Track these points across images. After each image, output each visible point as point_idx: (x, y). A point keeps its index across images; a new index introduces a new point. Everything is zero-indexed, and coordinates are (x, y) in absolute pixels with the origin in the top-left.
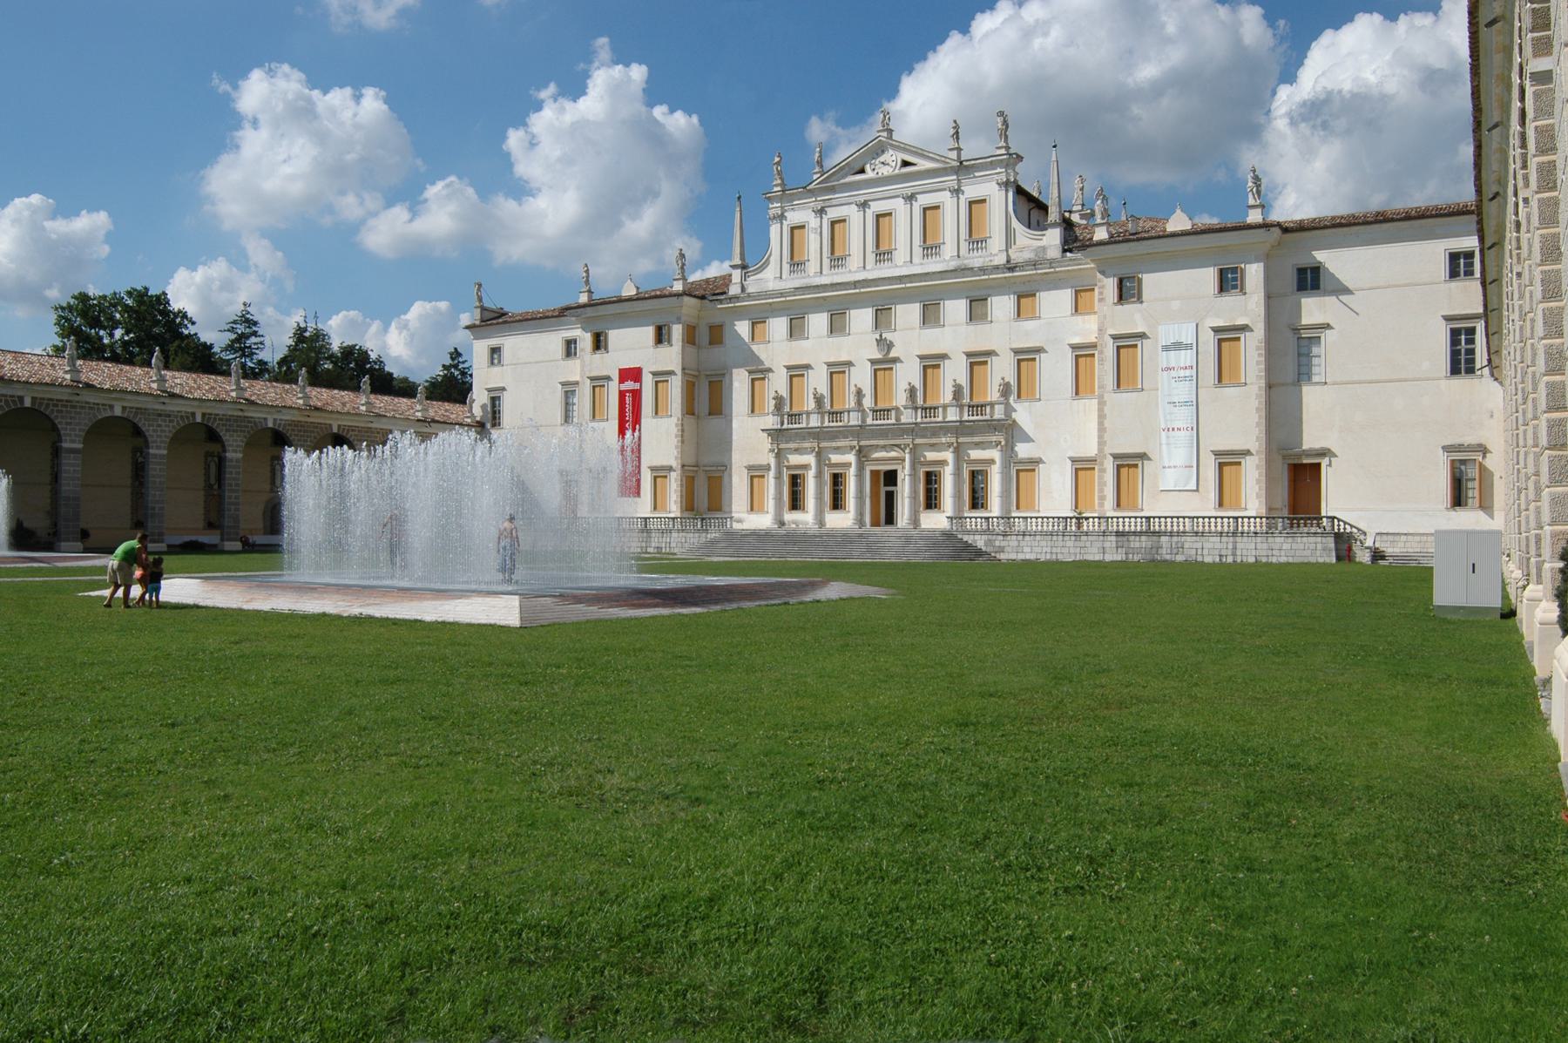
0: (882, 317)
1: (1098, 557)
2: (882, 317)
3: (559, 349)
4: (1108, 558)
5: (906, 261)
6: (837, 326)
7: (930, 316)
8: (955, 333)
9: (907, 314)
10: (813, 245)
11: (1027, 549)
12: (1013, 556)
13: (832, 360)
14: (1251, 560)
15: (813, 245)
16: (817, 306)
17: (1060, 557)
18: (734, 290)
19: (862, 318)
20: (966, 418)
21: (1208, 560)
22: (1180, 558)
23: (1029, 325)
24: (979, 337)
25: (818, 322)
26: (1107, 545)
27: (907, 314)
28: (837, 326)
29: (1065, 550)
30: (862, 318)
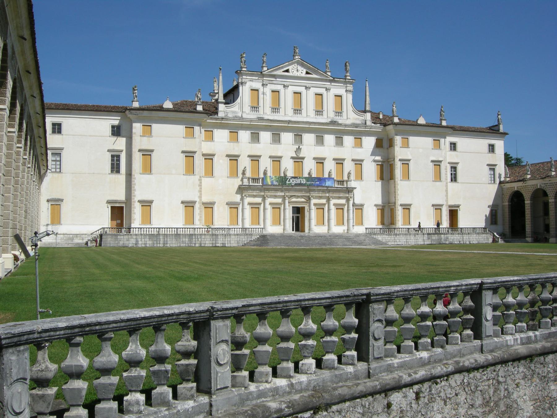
0: (298, 138)
1: (422, 243)
2: (298, 138)
3: (486, 149)
4: (426, 243)
5: (309, 115)
6: (276, 139)
7: (320, 141)
8: (329, 149)
9: (309, 138)
10: (266, 100)
11: (398, 241)
12: (393, 243)
13: (273, 155)
14: (468, 243)
15: (266, 100)
16: (266, 128)
17: (410, 243)
18: (221, 114)
19: (287, 138)
20: (336, 186)
21: (456, 243)
22: (447, 242)
23: (359, 150)
24: (340, 153)
25: (266, 136)
26: (425, 238)
27: (309, 138)
28: (276, 139)
29: (411, 241)
30: (287, 138)
